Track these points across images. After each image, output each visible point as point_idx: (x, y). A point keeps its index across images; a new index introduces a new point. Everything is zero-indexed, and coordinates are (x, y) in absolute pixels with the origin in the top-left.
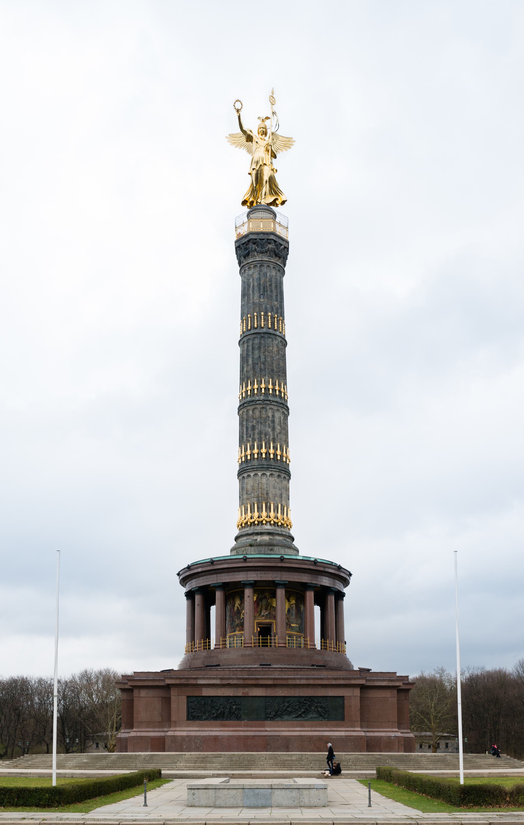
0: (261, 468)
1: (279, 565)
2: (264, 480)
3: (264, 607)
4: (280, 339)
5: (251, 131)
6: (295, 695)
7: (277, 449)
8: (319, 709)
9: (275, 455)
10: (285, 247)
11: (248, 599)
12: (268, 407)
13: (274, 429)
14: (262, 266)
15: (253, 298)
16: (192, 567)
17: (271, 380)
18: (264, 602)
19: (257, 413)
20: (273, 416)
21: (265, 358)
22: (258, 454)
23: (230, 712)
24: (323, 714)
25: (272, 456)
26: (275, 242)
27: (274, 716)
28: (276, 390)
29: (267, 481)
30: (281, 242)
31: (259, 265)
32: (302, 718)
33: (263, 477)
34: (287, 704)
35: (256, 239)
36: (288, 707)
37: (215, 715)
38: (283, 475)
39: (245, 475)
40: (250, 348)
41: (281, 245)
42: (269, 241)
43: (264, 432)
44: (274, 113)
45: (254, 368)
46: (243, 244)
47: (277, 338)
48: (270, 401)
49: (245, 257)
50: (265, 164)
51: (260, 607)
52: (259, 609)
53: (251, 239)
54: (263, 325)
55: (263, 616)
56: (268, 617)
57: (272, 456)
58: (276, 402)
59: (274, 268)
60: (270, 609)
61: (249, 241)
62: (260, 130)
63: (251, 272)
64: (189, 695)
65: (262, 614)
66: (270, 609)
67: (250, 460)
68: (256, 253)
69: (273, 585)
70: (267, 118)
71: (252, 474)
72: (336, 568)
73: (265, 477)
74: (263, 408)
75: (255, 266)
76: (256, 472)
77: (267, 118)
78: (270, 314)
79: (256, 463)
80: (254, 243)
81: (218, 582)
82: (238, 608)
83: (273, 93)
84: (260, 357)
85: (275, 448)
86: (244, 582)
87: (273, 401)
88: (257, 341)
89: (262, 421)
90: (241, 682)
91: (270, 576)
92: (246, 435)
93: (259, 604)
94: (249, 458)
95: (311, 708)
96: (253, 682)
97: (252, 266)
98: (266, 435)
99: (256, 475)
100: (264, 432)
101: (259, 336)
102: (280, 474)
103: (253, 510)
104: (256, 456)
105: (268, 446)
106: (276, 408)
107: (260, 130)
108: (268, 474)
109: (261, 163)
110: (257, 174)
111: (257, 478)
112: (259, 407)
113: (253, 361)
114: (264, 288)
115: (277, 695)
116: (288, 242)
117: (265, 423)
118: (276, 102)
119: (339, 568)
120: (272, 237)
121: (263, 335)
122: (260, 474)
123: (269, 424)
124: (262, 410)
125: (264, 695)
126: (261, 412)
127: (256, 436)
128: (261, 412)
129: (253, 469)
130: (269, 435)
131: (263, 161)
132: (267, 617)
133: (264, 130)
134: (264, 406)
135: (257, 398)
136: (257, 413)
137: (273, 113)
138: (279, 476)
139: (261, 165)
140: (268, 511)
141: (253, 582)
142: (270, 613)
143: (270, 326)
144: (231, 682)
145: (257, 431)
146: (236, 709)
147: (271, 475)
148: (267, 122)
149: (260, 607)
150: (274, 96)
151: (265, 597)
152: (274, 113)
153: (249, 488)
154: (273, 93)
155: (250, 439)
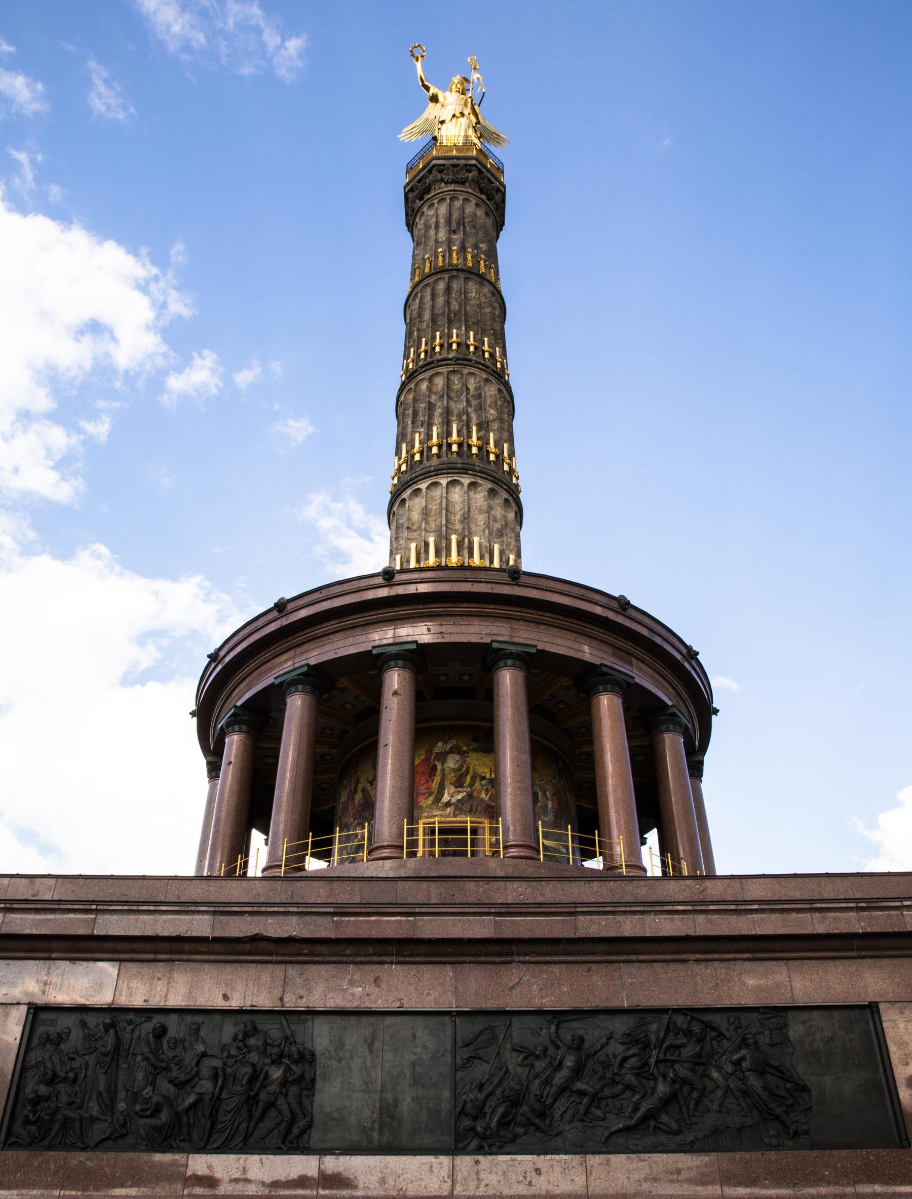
0: (447, 468)
1: (506, 590)
2: (457, 495)
3: (452, 777)
4: (492, 289)
6: (614, 1004)
7: (488, 443)
8: (755, 1082)
9: (483, 450)
10: (498, 191)
11: (395, 700)
12: (466, 371)
13: (480, 408)
14: (453, 199)
15: (436, 234)
16: (222, 654)
17: (472, 333)
18: (452, 762)
19: (440, 382)
20: (478, 388)
21: (460, 305)
22: (440, 446)
23: (251, 1100)
24: (779, 1111)
25: (474, 450)
26: (480, 172)
27: (504, 1123)
28: (483, 352)
29: (461, 496)
30: (493, 180)
31: (448, 198)
32: (663, 1138)
33: (452, 489)
34: (569, 1062)
35: (443, 165)
36: (578, 1071)
37: (164, 1116)
38: (505, 495)
39: (406, 494)
40: (428, 298)
41: (492, 183)
42: (468, 168)
43: (455, 412)
45: (434, 319)
46: (419, 181)
47: (485, 282)
48: (470, 360)
49: (421, 199)
51: (437, 779)
52: (435, 786)
53: (435, 165)
54: (455, 262)
55: (448, 804)
56: (466, 807)
57: (474, 450)
58: (483, 365)
59: (477, 205)
60: (471, 785)
61: (430, 171)
63: (432, 212)
64: (40, 1000)
65: (446, 798)
66: (471, 785)
67: (421, 462)
68: (443, 185)
69: (487, 658)
71: (423, 486)
72: (684, 651)
73: (457, 489)
74: (454, 372)
75: (442, 200)
76: (433, 479)
78: (470, 250)
79: (435, 462)
80: (441, 172)
81: (296, 666)
82: (364, 790)
84: (448, 303)
85: (484, 440)
86: (381, 650)
87: (480, 363)
88: (441, 286)
89: (453, 395)
90: (323, 928)
91: (471, 629)
92: (413, 422)
93: (434, 768)
94: (417, 457)
95: (706, 1075)
96: (391, 926)
97: (436, 201)
98: (459, 416)
99: (435, 484)
100: (455, 412)
101: (446, 276)
102: (496, 487)
103: (423, 555)
104: (435, 450)
105: (465, 431)
106: (485, 376)
108: (466, 480)
111: (437, 493)
112: (444, 370)
113: (433, 310)
114: (458, 224)
115: (514, 1002)
116: (504, 187)
117: (459, 398)
119: (692, 655)
120: (474, 162)
121: (454, 273)
122: (444, 481)
123: (468, 401)
124: (452, 377)
125: (449, 1002)
126: (448, 379)
127: (437, 419)
128: (448, 379)
129: (426, 475)
130: (468, 416)
132: (459, 807)
134: (456, 368)
135: (438, 357)
136: (440, 382)
138: (492, 493)
140: (466, 555)
141: (414, 646)
142: (470, 796)
143: (470, 264)
144: (274, 927)
145: (438, 412)
146: (284, 1082)
147: (473, 485)
149: (437, 779)
151: (455, 750)
153: (416, 516)
155: (422, 430)
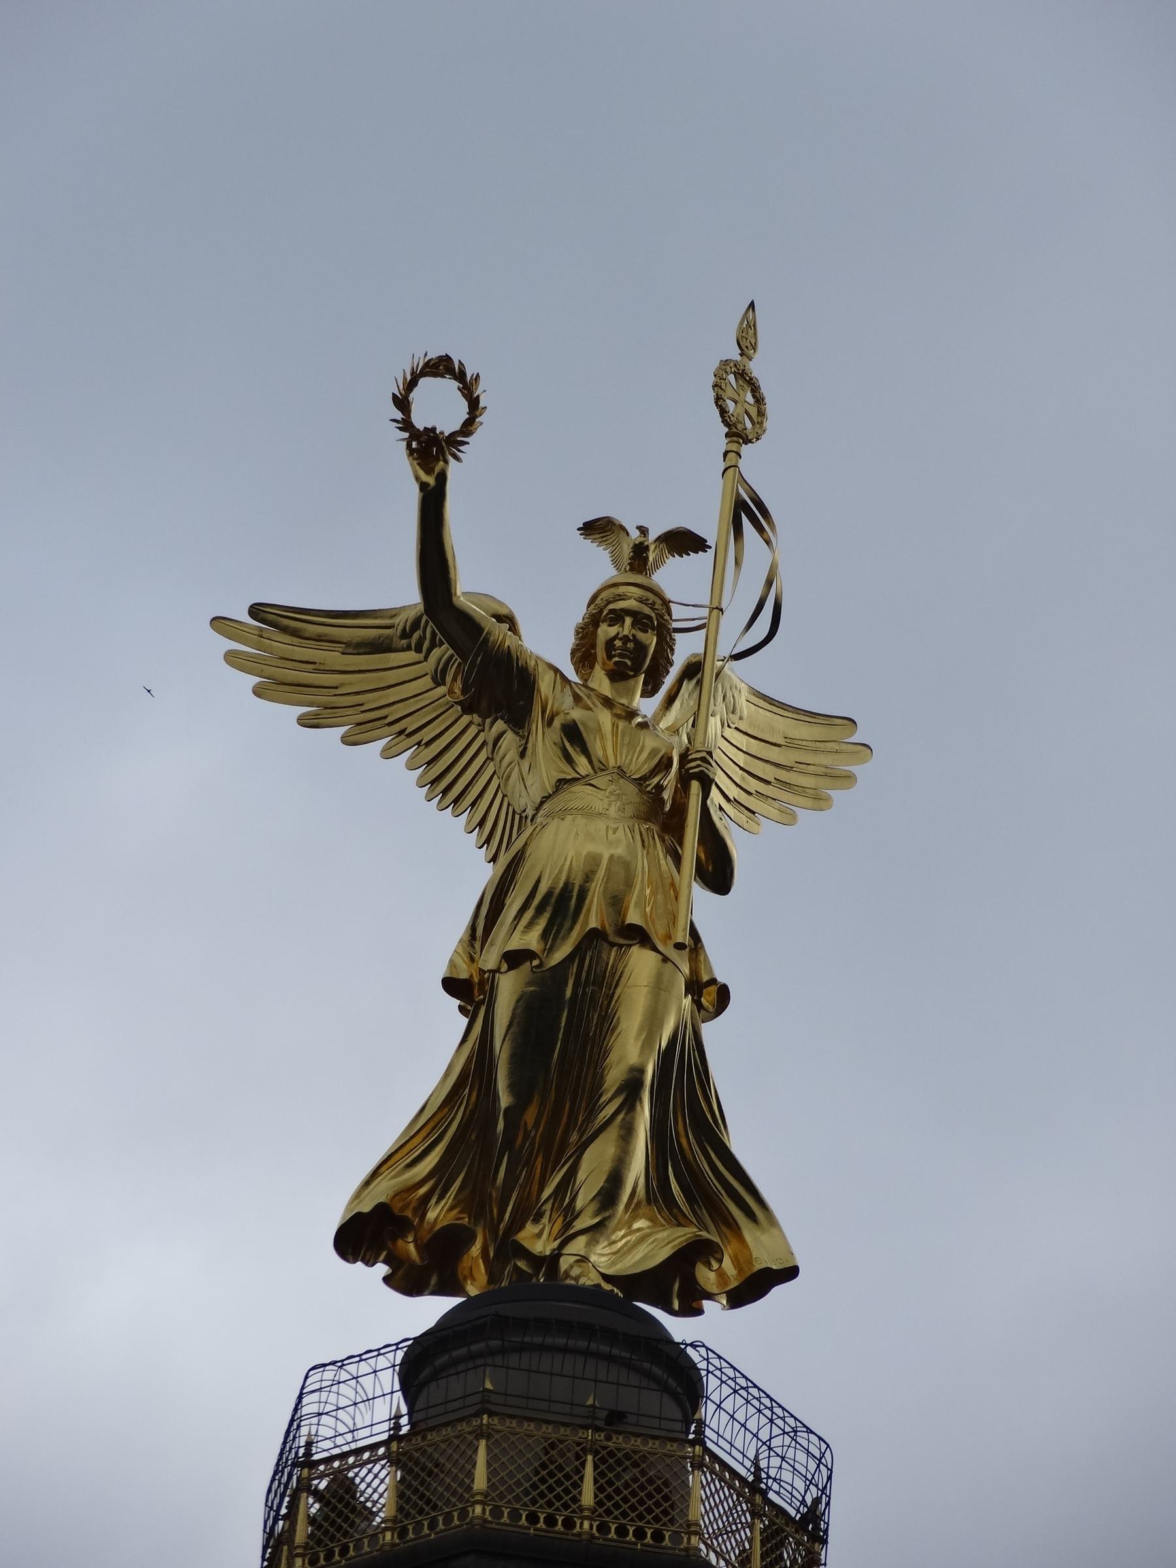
5: (508, 620)
44: (748, 511)
50: (640, 936)
62: (606, 631)
70: (683, 542)
77: (683, 542)
83: (747, 341)
107: (606, 631)
109: (594, 917)
110: (535, 1013)
118: (771, 423)
131: (617, 903)
133: (651, 641)
137: (740, 507)
139: (595, 936)
148: (679, 578)
150: (756, 368)
152: (748, 511)
154: (747, 341)
